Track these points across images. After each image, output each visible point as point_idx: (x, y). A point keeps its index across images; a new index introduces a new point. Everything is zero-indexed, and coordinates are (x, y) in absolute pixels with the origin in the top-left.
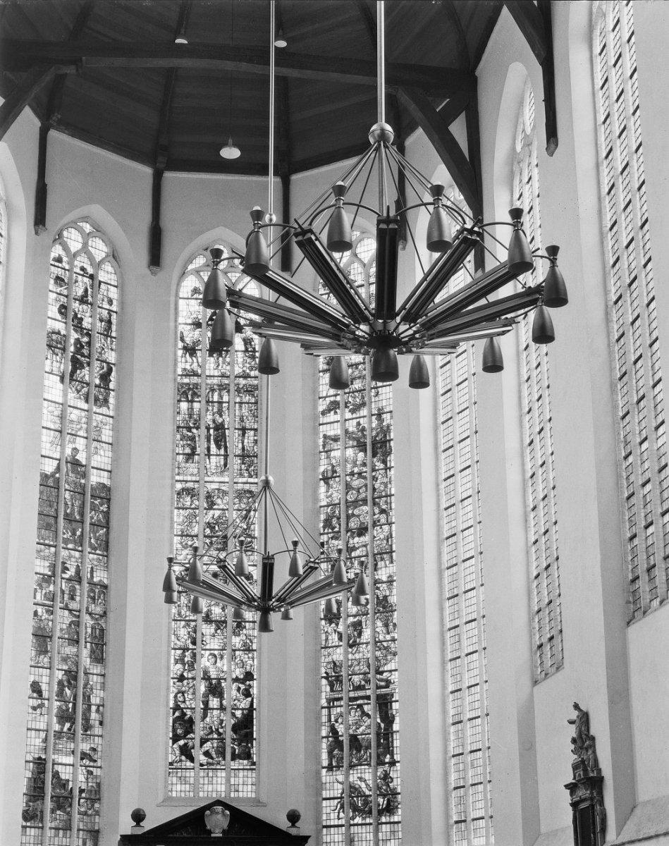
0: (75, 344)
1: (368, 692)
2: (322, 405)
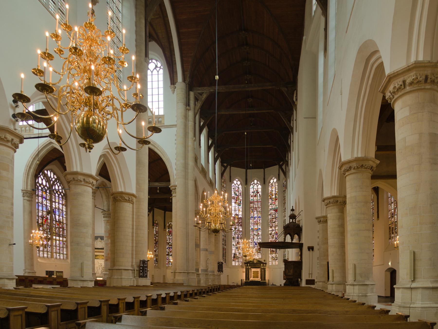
2: (269, 204)
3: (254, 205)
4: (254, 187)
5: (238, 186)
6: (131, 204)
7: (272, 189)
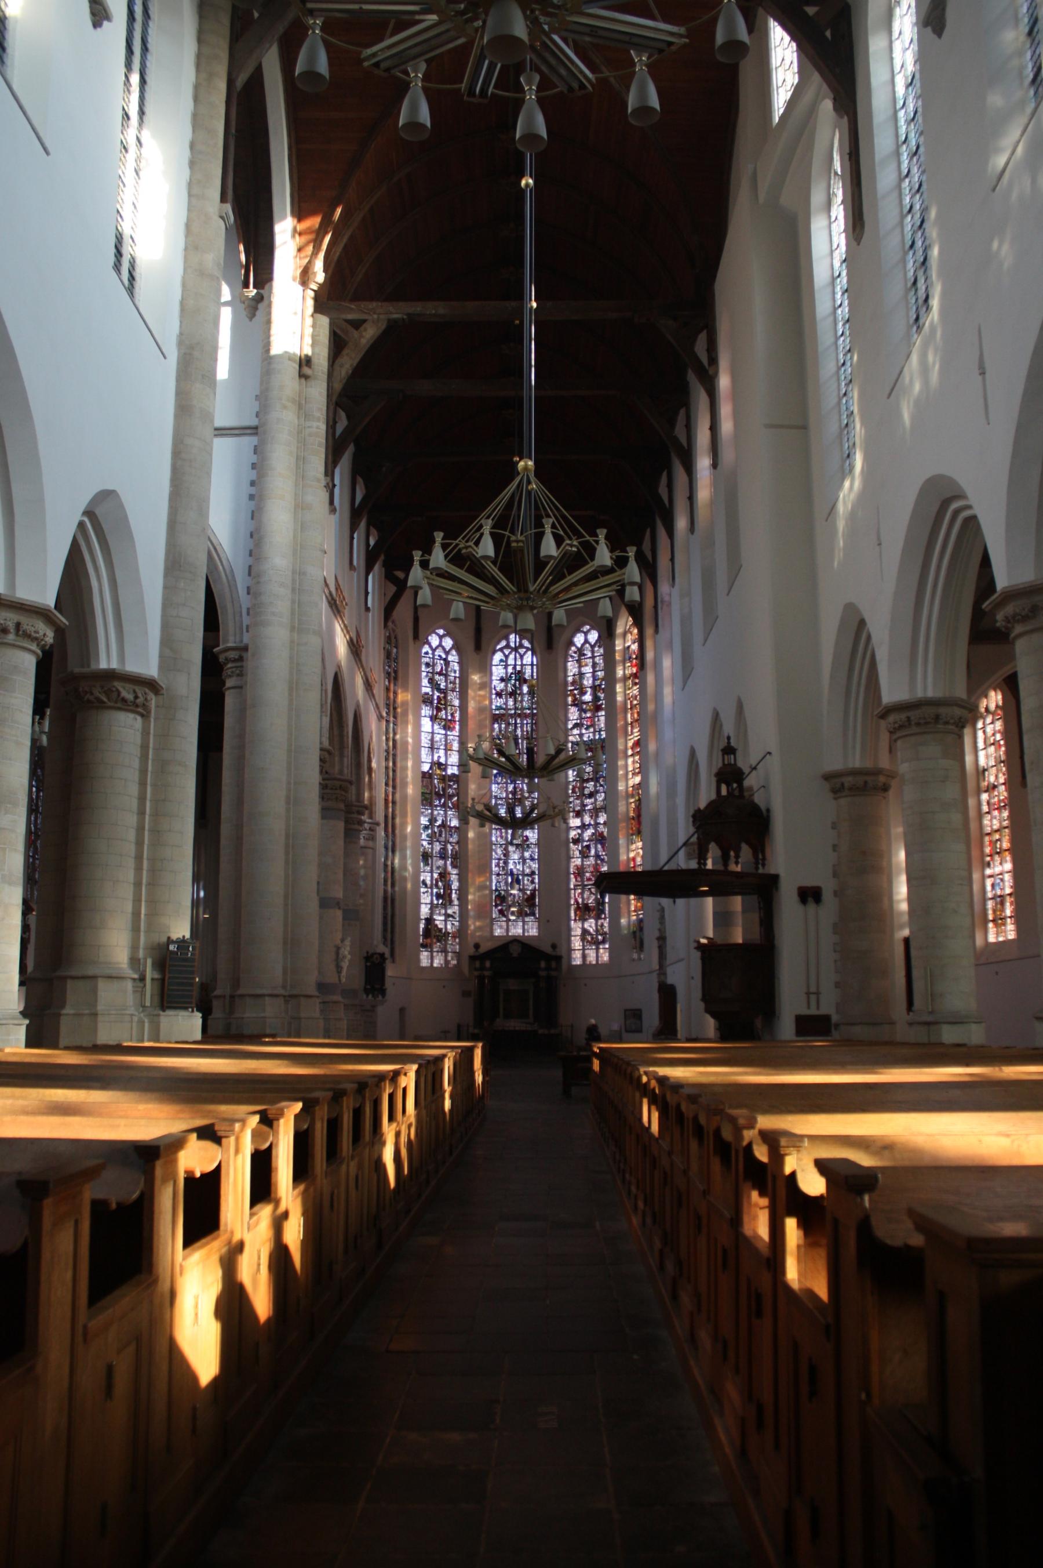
0: (437, 699)
2: (570, 726)
3: (506, 728)
4: (506, 661)
6: (139, 718)
7: (580, 666)
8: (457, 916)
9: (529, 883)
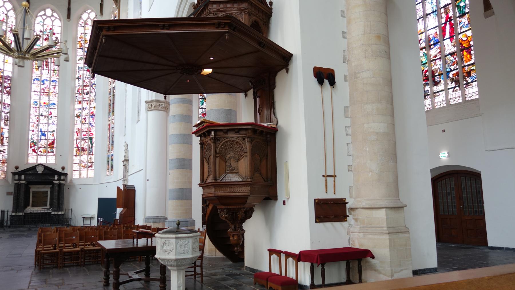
1: (87, 137)
2: (78, 58)
4: (44, 22)
5: (6, 13)
7: (85, 30)
8: (6, 152)
9: (51, 136)
